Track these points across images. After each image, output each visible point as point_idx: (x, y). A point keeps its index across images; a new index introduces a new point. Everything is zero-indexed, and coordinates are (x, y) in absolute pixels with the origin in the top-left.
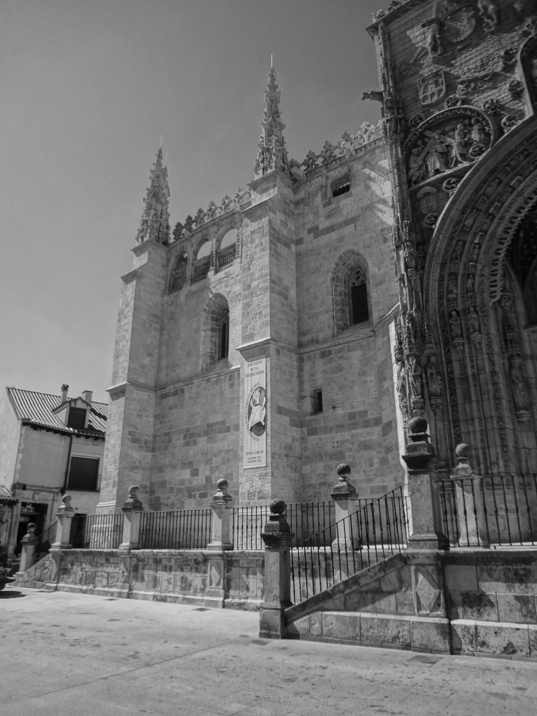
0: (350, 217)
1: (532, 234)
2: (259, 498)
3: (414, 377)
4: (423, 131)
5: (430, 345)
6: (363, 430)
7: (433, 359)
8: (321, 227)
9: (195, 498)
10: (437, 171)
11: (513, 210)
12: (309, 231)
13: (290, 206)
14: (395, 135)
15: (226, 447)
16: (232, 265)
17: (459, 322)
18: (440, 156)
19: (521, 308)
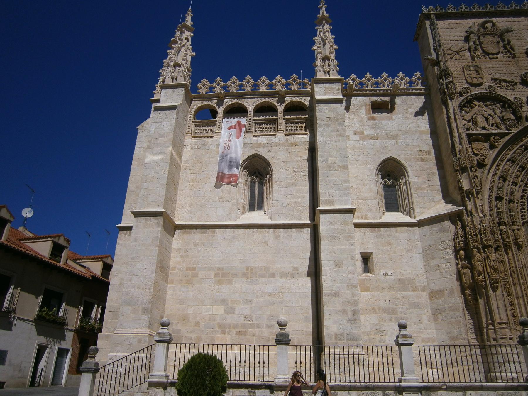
0: (391, 134)
2: (348, 340)
4: (473, 99)
6: (413, 293)
8: (366, 133)
9: (229, 334)
10: (484, 128)
12: (355, 133)
15: (270, 291)
16: (275, 135)
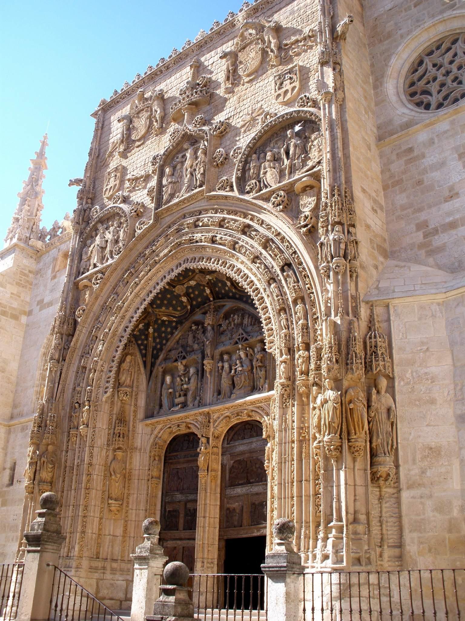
1: (163, 329)
3: (31, 464)
5: (48, 435)
7: (50, 448)
11: (132, 310)
13: (28, 276)
14: (78, 225)
17: (77, 414)
18: (100, 250)
19: (142, 402)
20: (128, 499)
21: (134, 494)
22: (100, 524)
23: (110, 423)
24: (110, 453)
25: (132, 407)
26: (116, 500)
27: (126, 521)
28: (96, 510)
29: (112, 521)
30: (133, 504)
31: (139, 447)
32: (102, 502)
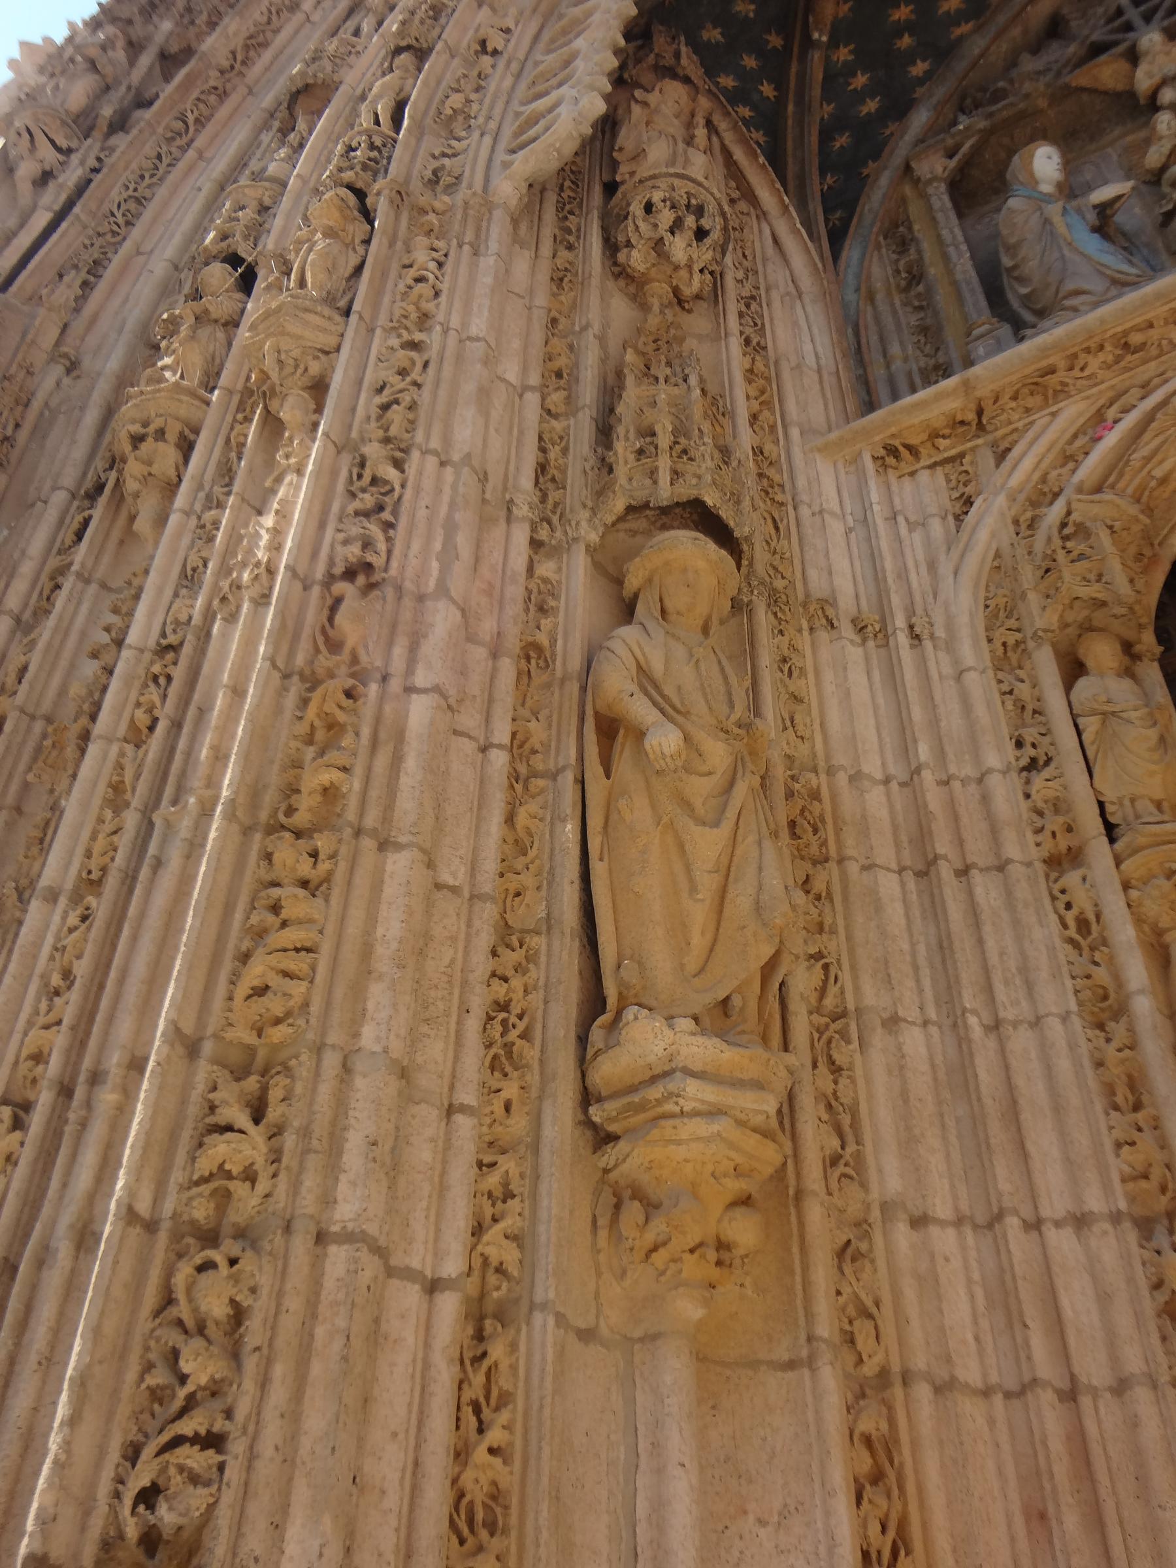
19: (804, 336)
20: (836, 1070)
21: (893, 1022)
22: (476, 1411)
23: (559, 376)
24: (576, 579)
25: (735, 344)
26: (720, 1017)
27: (873, 1388)
28: (423, 1154)
29: (674, 1370)
30: (909, 1143)
31: (846, 604)
32: (501, 1062)
